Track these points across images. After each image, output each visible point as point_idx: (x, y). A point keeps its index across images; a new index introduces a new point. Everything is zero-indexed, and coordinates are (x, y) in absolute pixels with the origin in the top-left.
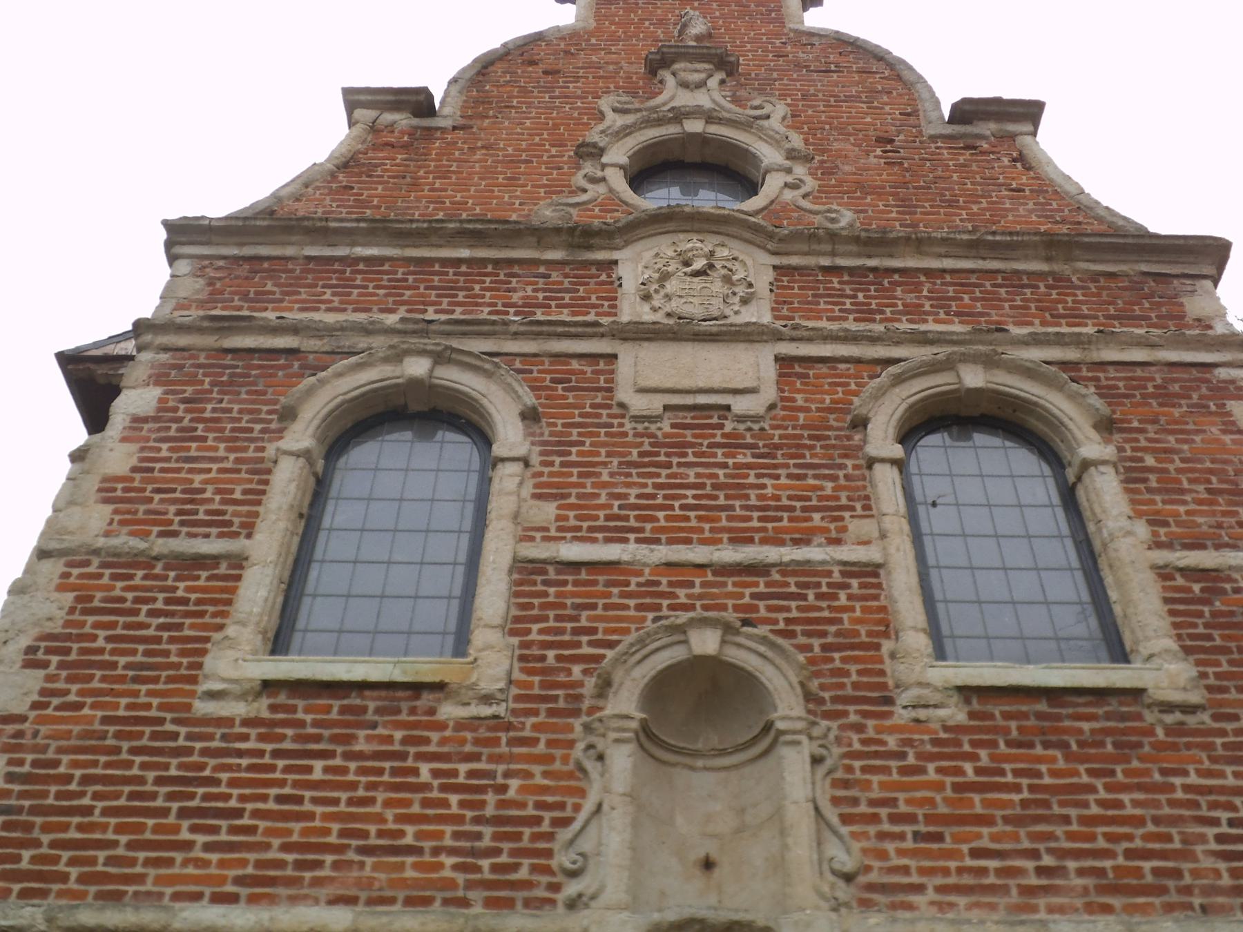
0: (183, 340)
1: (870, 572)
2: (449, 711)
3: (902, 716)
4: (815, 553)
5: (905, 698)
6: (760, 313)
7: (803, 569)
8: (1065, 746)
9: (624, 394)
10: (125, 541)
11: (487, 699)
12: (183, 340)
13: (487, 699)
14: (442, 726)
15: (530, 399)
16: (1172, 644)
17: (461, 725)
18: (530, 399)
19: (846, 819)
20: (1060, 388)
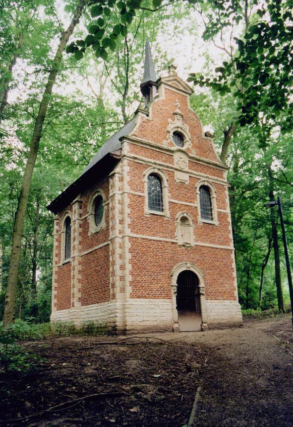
1: (196, 207)
2: (165, 219)
3: (198, 224)
4: (192, 204)
5: (199, 222)
6: (187, 169)
7: (191, 206)
10: (132, 192)
11: (168, 218)
13: (168, 218)
17: (167, 220)
18: (168, 178)
20: (213, 186)
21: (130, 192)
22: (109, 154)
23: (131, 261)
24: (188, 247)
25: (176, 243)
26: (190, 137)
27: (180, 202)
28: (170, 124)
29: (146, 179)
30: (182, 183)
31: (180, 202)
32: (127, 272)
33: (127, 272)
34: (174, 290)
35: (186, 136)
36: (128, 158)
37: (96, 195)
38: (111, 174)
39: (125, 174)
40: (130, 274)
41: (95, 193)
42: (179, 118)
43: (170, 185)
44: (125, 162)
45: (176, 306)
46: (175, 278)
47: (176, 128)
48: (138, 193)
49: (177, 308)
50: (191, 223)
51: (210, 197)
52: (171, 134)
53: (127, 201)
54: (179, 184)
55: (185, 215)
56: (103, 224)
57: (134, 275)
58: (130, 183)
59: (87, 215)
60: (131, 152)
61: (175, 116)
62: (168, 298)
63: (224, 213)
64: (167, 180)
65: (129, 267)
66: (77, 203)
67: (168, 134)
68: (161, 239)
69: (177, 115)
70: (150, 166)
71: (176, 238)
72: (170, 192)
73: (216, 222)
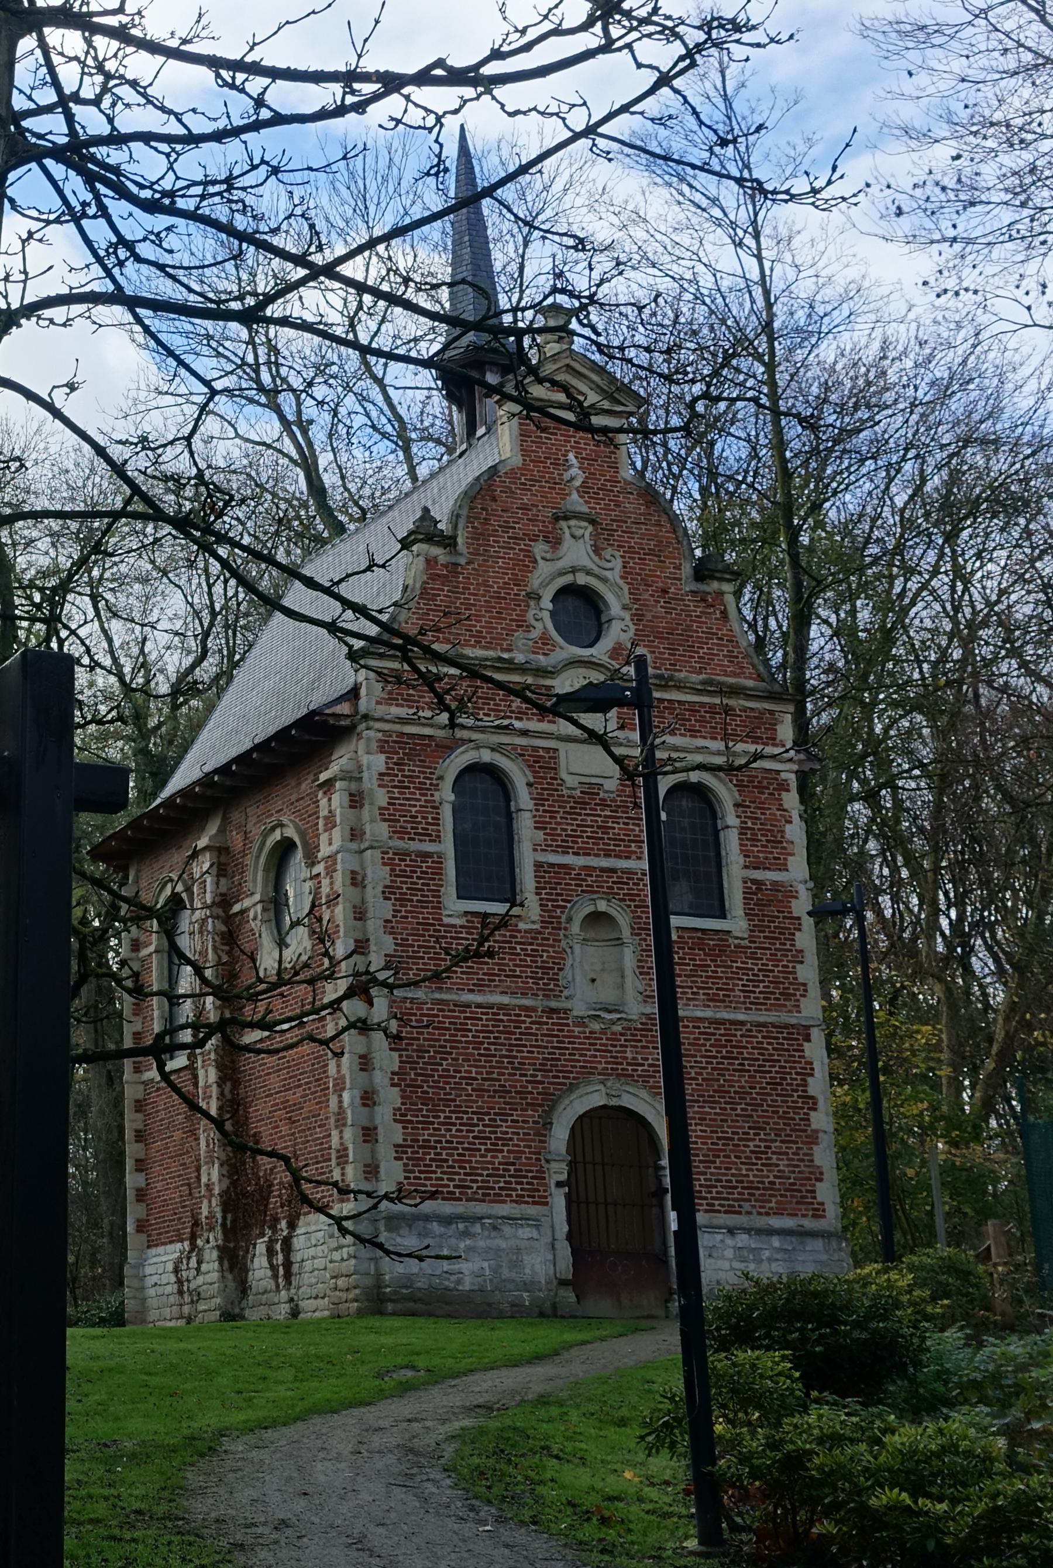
0: (387, 727)
7: (629, 872)
8: (703, 950)
9: (564, 775)
11: (533, 922)
12: (387, 727)
13: (533, 922)
14: (520, 931)
15: (532, 780)
16: (742, 913)
19: (641, 973)
21: (391, 843)
22: (312, 713)
23: (398, 1079)
24: (613, 1023)
25: (566, 1011)
26: (626, 598)
27: (580, 861)
28: (541, 562)
29: (446, 794)
30: (591, 791)
31: (580, 861)
32: (384, 1114)
33: (384, 1114)
34: (558, 1171)
35: (610, 597)
36: (378, 725)
37: (277, 835)
38: (323, 777)
39: (369, 781)
40: (395, 1120)
41: (273, 829)
42: (579, 533)
43: (539, 801)
44: (371, 734)
45: (566, 1229)
46: (560, 1136)
47: (562, 573)
48: (415, 846)
49: (569, 1237)
50: (626, 932)
51: (715, 825)
52: (547, 603)
53: (377, 874)
54: (578, 793)
55: (602, 906)
56: (300, 942)
57: (411, 1122)
58: (387, 815)
59: (247, 903)
60: (390, 700)
61: (563, 524)
62: (535, 1203)
63: (775, 883)
64: (529, 785)
65: (390, 1097)
66: (208, 855)
67: (532, 603)
68: (505, 1000)
69: (573, 522)
70: (464, 741)
71: (566, 993)
72: (540, 826)
73: (737, 923)
